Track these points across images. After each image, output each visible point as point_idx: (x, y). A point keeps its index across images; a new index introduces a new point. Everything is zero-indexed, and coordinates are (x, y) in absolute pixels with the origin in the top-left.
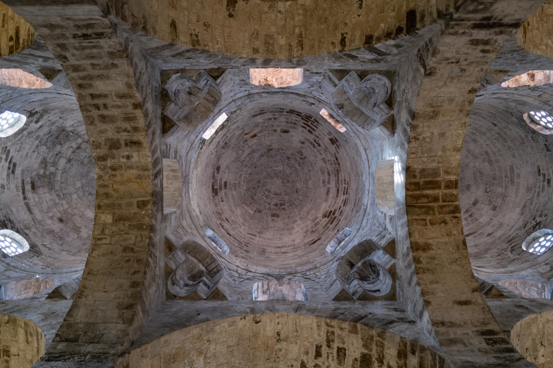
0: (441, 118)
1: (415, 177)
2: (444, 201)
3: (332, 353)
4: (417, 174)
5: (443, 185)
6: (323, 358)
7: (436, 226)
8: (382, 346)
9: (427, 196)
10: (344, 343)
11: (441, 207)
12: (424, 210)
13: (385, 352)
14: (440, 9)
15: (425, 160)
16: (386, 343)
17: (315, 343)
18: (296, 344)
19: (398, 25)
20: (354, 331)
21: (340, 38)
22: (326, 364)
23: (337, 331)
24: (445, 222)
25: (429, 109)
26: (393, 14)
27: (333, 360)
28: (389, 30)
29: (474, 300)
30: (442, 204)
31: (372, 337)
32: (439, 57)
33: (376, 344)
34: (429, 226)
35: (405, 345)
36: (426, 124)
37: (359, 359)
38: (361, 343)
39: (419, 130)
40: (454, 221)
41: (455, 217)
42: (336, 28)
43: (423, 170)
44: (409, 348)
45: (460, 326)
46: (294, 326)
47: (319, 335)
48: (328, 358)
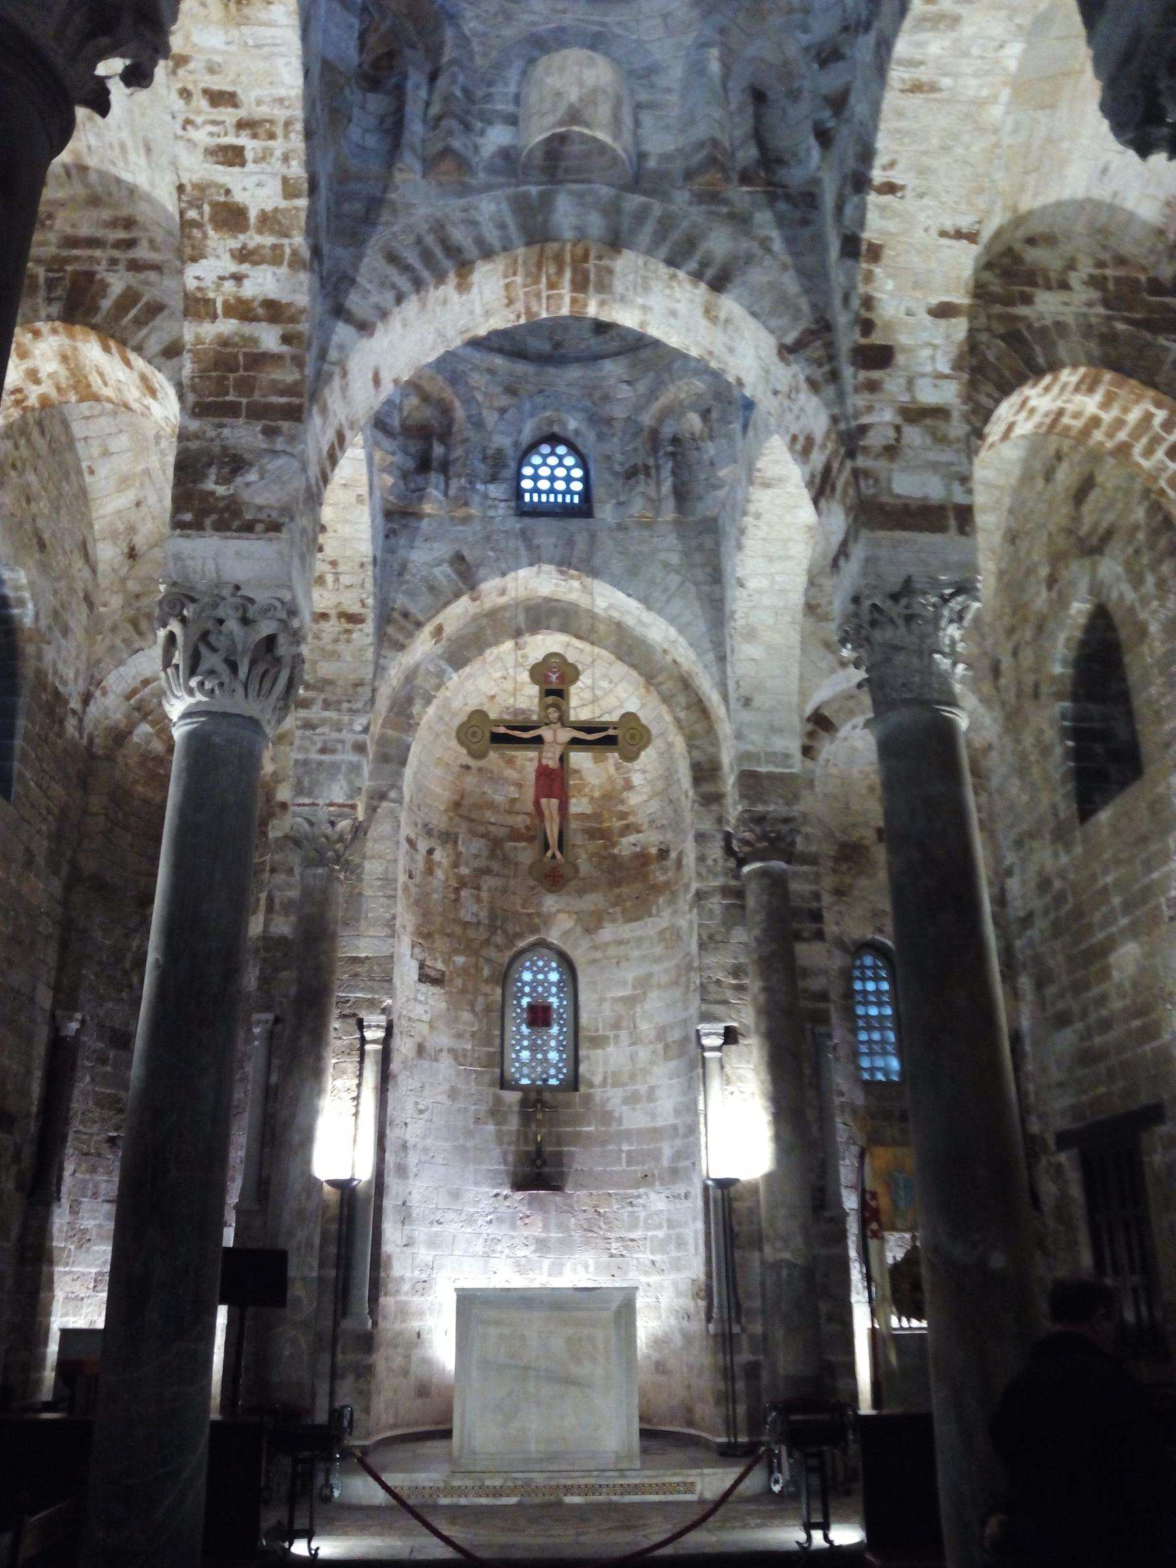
0: (703, 322)
1: (600, 258)
2: (549, 297)
3: (226, 134)
4: (605, 262)
5: (581, 296)
6: (210, 110)
7: (503, 293)
8: (276, 261)
9: (560, 272)
10: (255, 162)
11: (538, 295)
12: (534, 270)
13: (264, 266)
14: (871, 433)
15: (631, 277)
16: (284, 270)
17: (239, 92)
18: (228, 43)
19: (877, 321)
20: (289, 189)
21: (899, 182)
22: (199, 120)
23: (278, 146)
24: (510, 302)
25: (722, 315)
26: (902, 309)
27: (212, 134)
28: (875, 303)
29: (382, 389)
30: (544, 294)
31: (287, 236)
32: (804, 386)
33: (274, 247)
34: (503, 282)
35: (293, 319)
36: (698, 300)
37: (230, 200)
38: (269, 208)
39: (688, 286)
40: (512, 317)
41: (518, 317)
42: (923, 172)
43: (610, 271)
44: (290, 327)
45: (344, 397)
46: (269, 41)
47: (259, 103)
48: (215, 123)
